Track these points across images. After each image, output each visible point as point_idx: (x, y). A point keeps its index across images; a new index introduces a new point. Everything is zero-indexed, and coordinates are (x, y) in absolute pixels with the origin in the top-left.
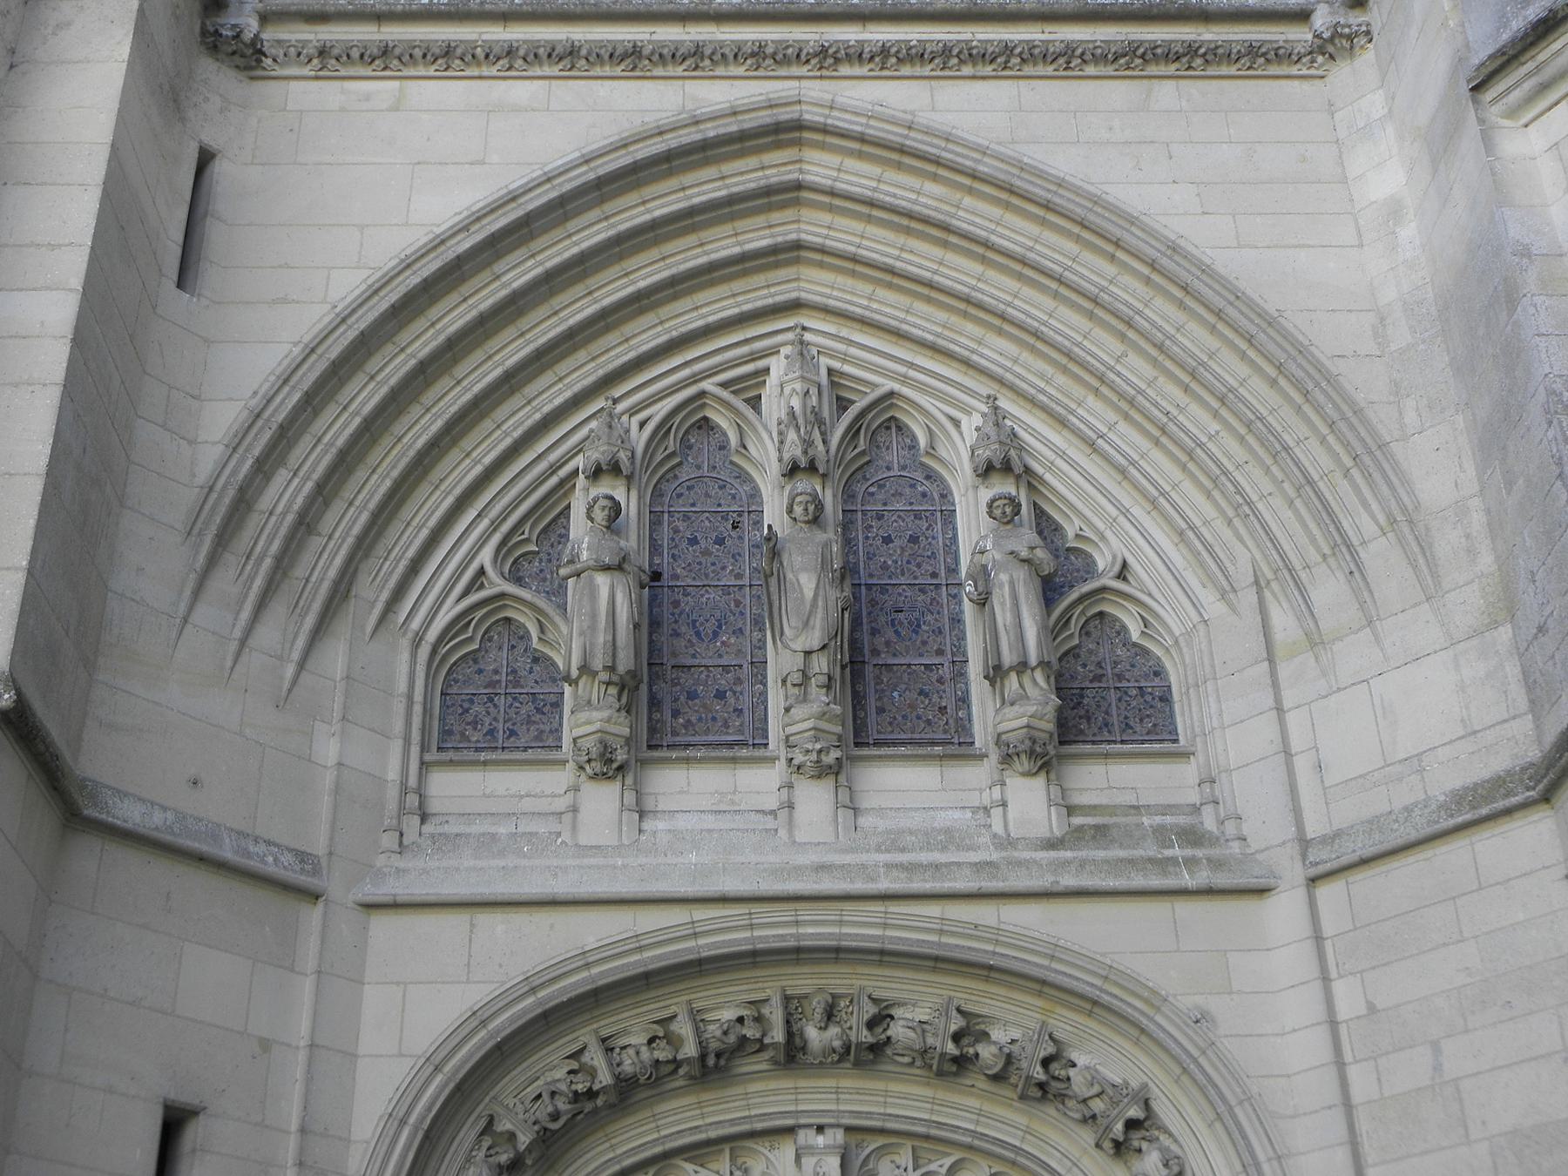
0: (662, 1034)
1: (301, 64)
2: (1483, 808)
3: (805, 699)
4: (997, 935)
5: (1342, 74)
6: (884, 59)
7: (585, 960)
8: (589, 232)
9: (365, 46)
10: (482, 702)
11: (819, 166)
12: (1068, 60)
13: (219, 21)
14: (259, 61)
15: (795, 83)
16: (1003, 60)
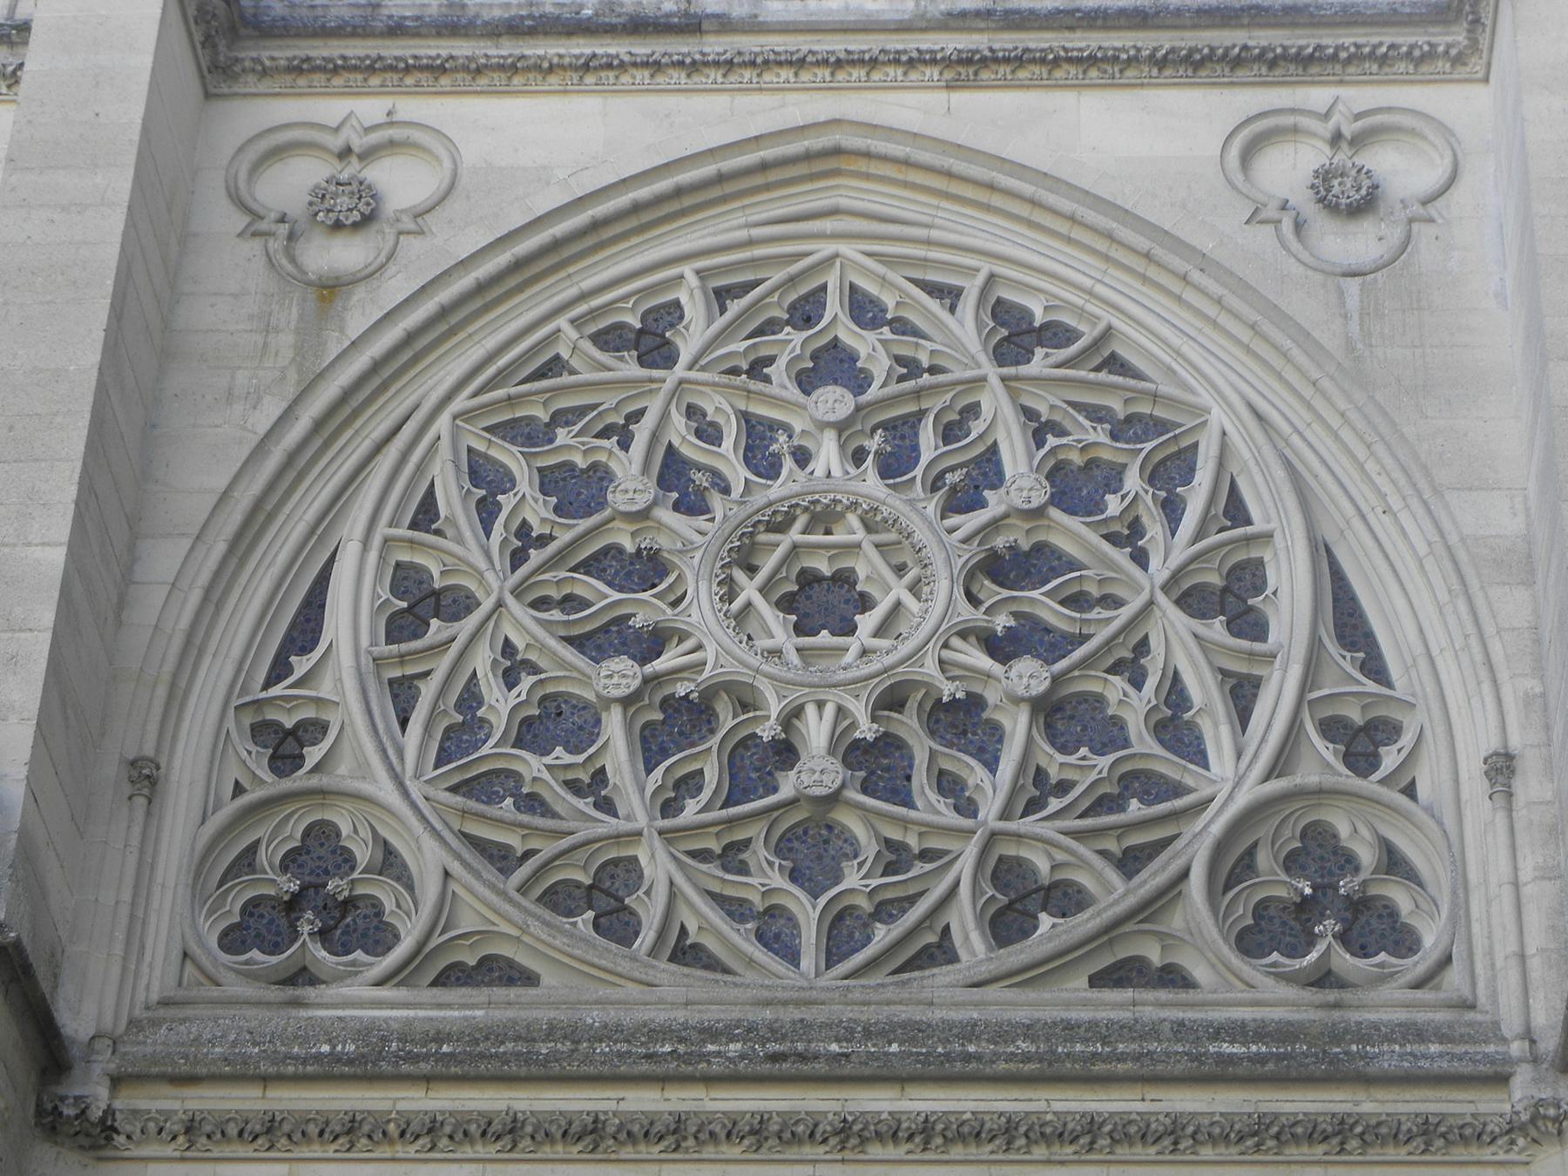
13: (61, 1091)
14: (109, 1139)
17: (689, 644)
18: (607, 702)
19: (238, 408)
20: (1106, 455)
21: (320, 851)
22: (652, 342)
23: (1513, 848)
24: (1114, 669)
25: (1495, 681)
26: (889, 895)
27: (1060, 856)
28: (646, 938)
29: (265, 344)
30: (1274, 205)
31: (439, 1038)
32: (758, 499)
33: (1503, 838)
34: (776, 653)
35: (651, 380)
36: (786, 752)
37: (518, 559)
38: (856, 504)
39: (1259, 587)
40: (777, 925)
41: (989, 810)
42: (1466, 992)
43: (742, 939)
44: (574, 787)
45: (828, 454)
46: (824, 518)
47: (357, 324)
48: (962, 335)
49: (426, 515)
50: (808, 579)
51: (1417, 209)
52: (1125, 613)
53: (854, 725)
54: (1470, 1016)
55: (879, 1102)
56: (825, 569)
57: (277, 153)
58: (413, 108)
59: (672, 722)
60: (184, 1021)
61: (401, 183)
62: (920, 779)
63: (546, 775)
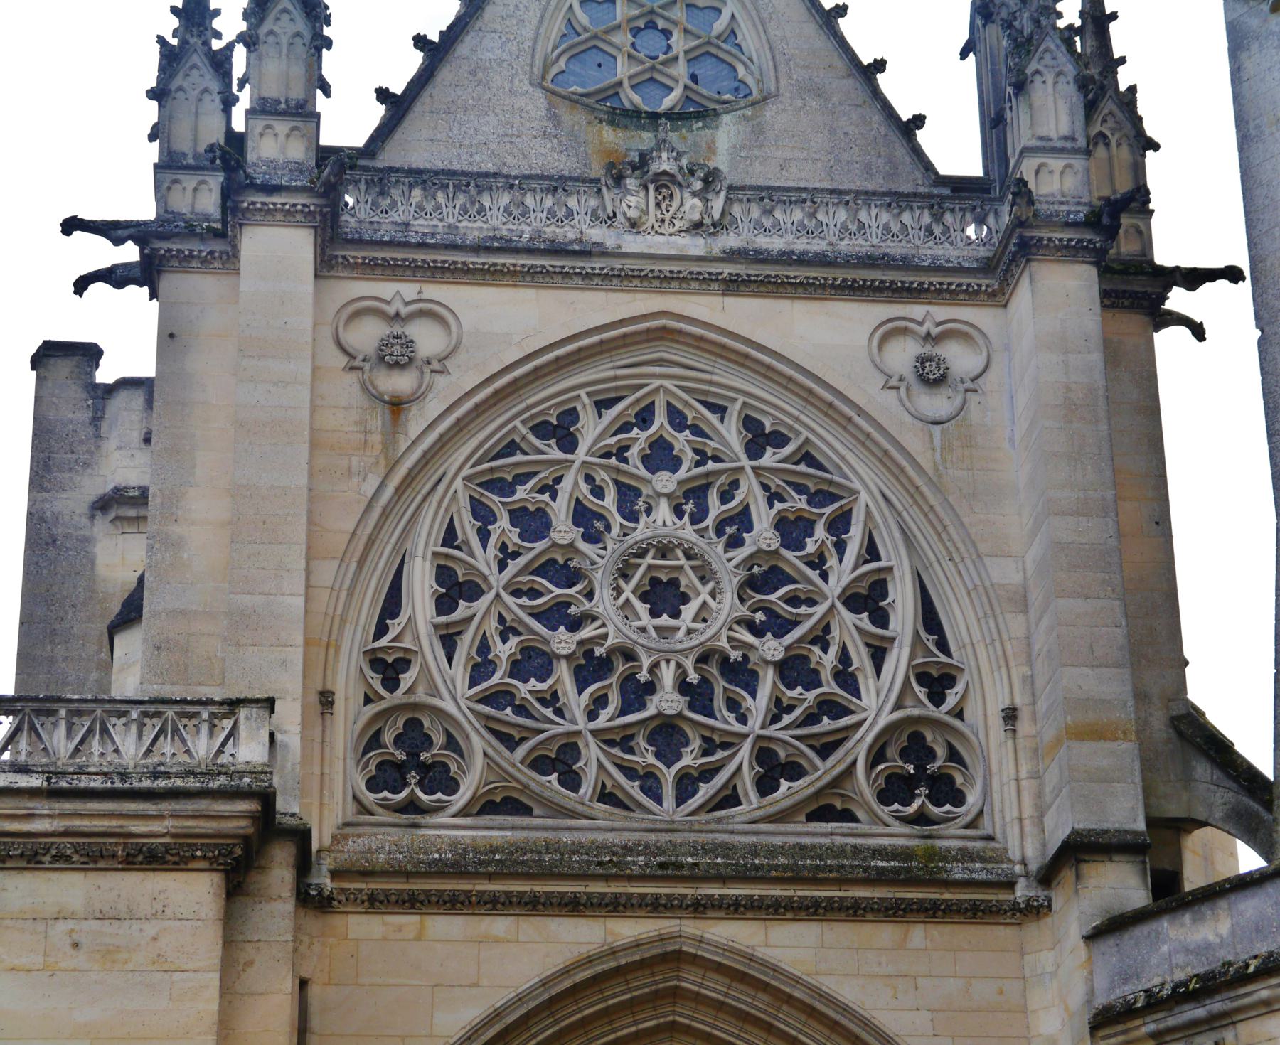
1: (358, 905)
5: (1034, 932)
6: (737, 909)
12: (855, 911)
15: (677, 922)
17: (598, 623)
18: (559, 657)
19: (355, 480)
20: (805, 515)
21: (414, 736)
22: (562, 431)
23: (1016, 759)
24: (813, 642)
25: (1007, 666)
26: (706, 768)
27: (791, 750)
28: (586, 789)
29: (366, 441)
30: (896, 378)
31: (494, 850)
32: (630, 540)
33: (1011, 755)
34: (643, 630)
35: (567, 461)
36: (650, 688)
37: (502, 566)
38: (681, 544)
39: (885, 595)
40: (650, 782)
42: (990, 832)
43: (633, 788)
44: (542, 701)
45: (663, 512)
47: (414, 429)
50: (655, 582)
51: (969, 385)
52: (820, 610)
53: (685, 674)
54: (992, 844)
55: (715, 890)
56: (665, 579)
57: (357, 314)
58: (434, 291)
59: (590, 667)
60: (359, 836)
61: (427, 339)
62: (719, 702)
63: (528, 696)
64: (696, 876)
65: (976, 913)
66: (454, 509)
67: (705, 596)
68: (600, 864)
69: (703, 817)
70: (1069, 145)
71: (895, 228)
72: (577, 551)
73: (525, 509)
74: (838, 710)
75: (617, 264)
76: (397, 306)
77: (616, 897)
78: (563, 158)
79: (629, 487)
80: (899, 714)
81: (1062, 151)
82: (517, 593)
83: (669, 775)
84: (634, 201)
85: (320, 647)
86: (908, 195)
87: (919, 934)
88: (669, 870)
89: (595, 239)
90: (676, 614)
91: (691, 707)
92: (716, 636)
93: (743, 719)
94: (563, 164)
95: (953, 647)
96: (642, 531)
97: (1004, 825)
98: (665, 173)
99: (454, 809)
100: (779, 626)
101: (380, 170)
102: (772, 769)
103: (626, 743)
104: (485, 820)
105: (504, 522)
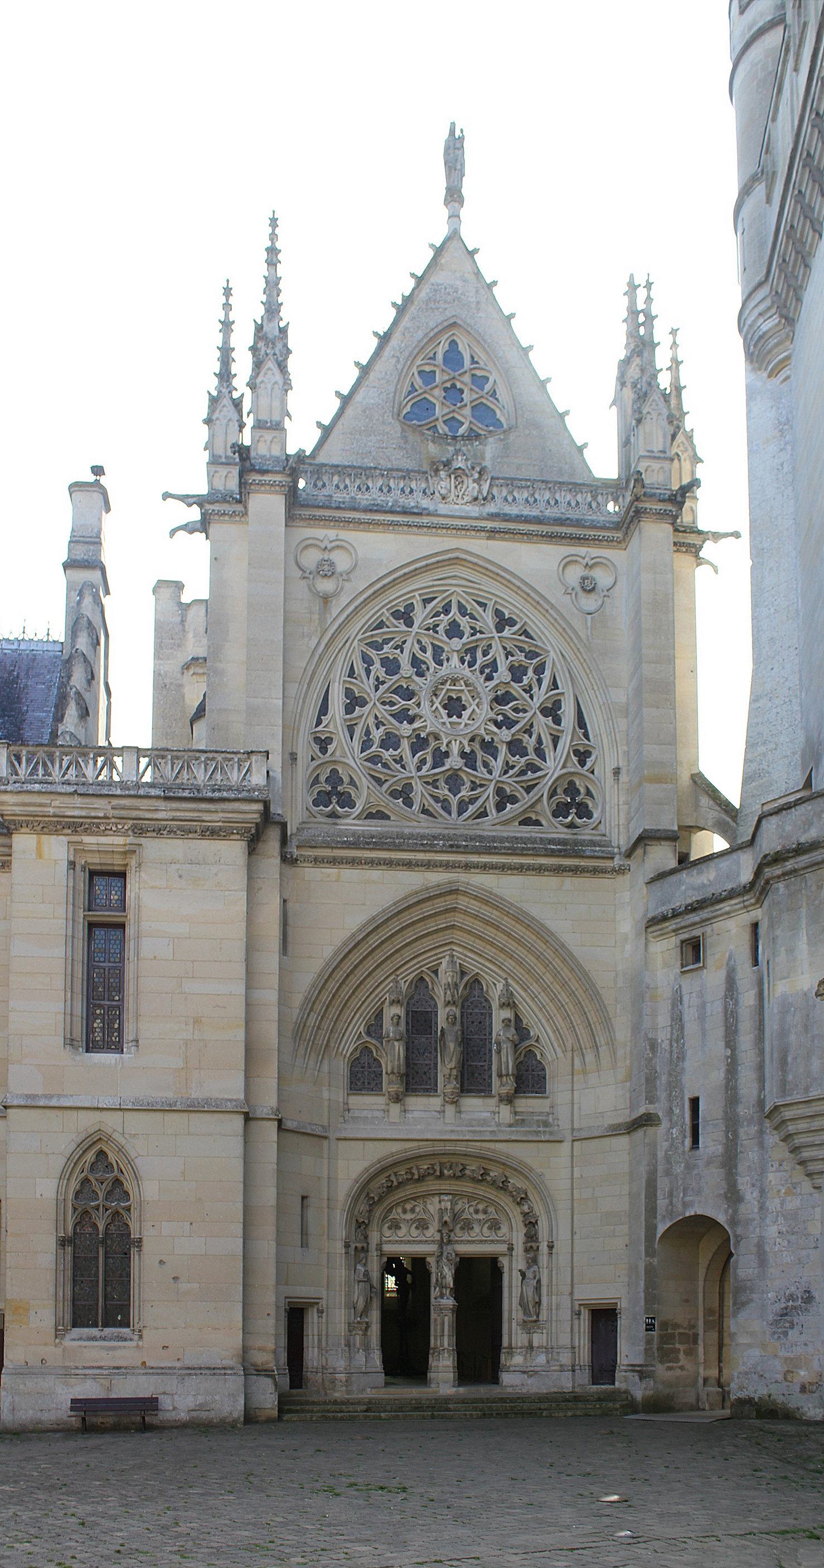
0: (409, 1172)
2: (616, 1131)
3: (449, 1082)
4: (494, 1151)
5: (622, 881)
6: (485, 867)
7: (392, 1155)
8: (395, 926)
9: (328, 857)
10: (363, 1076)
11: (463, 902)
12: (539, 870)
16: (521, 869)
18: (403, 737)
22: (406, 616)
24: (524, 732)
34: (444, 723)
36: (447, 754)
39: (560, 709)
41: (496, 773)
42: (604, 832)
46: (454, 681)
48: (488, 619)
49: (351, 673)
50: (450, 698)
52: (529, 715)
53: (464, 747)
54: (605, 838)
55: (474, 858)
59: (419, 743)
62: (479, 763)
64: (466, 851)
65: (595, 871)
66: (353, 657)
67: (474, 706)
68: (422, 844)
69: (470, 822)
70: (662, 455)
71: (573, 504)
72: (413, 681)
73: (388, 658)
74: (536, 769)
75: (435, 520)
76: (326, 543)
77: (429, 861)
78: (409, 461)
79: (439, 647)
80: (565, 771)
81: (659, 458)
82: (384, 703)
83: (454, 801)
84: (443, 484)
85: (289, 730)
86: (580, 485)
87: (569, 882)
88: (454, 848)
89: (424, 506)
90: (460, 716)
91: (466, 765)
92: (478, 728)
93: (490, 772)
94: (409, 464)
95: (591, 737)
96: (444, 671)
97: (610, 829)
98: (460, 468)
99: (354, 816)
100: (508, 723)
101: (317, 465)
102: (504, 799)
103: (434, 784)
104: (368, 822)
105: (377, 664)
